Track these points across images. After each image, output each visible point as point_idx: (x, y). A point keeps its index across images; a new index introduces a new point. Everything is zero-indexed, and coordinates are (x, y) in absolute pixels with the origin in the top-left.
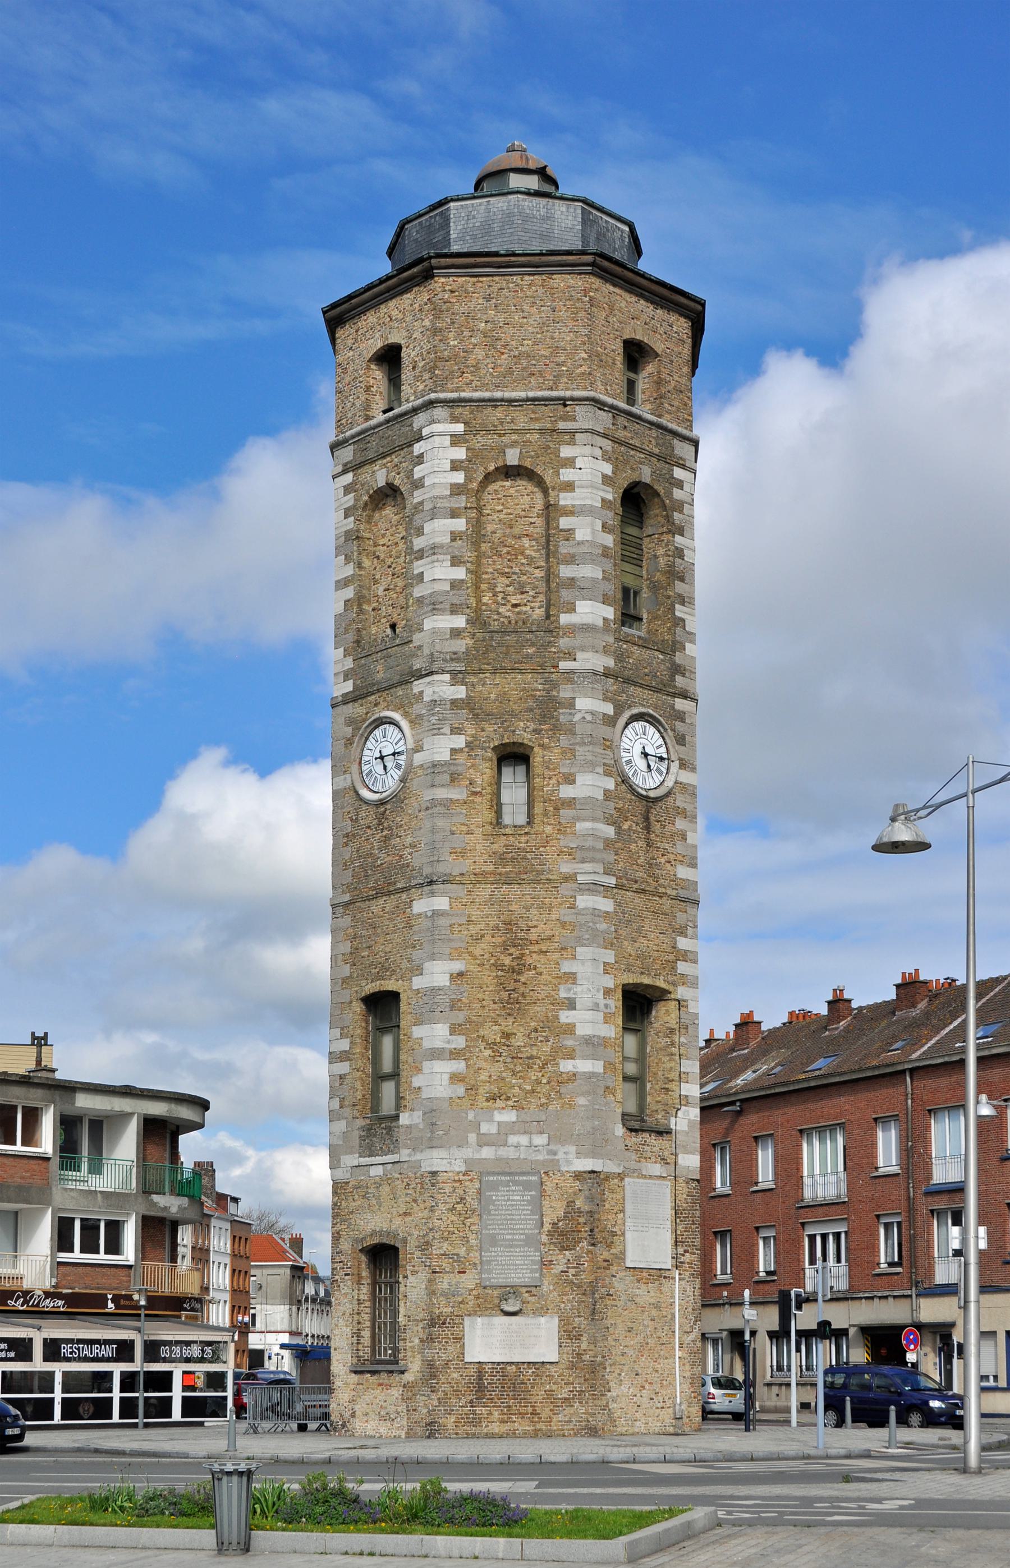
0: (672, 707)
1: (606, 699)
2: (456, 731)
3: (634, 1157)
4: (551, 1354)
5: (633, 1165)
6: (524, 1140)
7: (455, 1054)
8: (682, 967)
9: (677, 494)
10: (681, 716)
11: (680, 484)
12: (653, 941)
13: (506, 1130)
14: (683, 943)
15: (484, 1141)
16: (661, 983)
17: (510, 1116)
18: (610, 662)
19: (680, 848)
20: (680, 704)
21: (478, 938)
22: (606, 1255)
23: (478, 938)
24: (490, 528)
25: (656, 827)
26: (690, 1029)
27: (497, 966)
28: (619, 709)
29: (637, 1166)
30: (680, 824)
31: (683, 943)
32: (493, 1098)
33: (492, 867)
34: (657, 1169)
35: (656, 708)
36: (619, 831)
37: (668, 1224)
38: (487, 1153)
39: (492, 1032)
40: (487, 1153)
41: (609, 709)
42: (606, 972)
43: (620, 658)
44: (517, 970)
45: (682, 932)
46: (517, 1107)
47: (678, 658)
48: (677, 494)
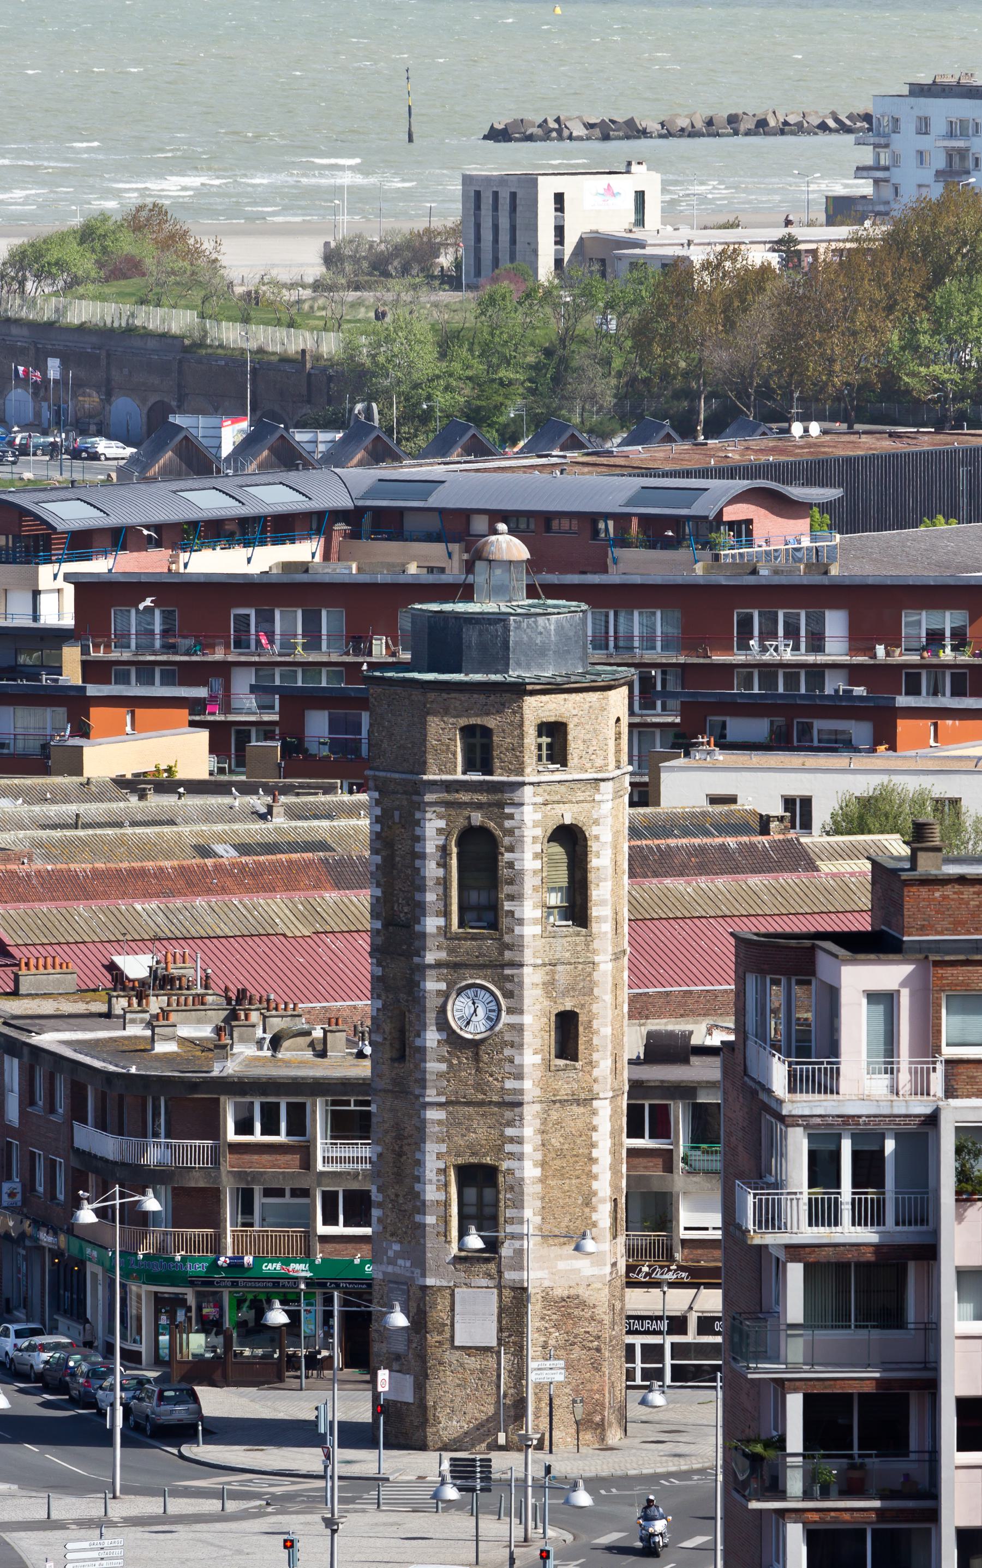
0: (502, 974)
1: (438, 980)
2: (379, 997)
3: (463, 1274)
4: (411, 1400)
5: (463, 1280)
6: (400, 1262)
7: (380, 1205)
8: (508, 1148)
9: (508, 824)
10: (510, 979)
11: (511, 817)
12: (481, 1132)
13: (398, 1255)
14: (509, 1132)
15: (392, 1262)
16: (488, 1160)
17: (396, 1247)
18: (443, 955)
19: (507, 1067)
20: (508, 972)
21: (387, 1132)
22: (438, 1338)
23: (387, 1132)
24: (398, 859)
25: (485, 1058)
26: (516, 1189)
27: (393, 1150)
28: (450, 985)
29: (468, 1281)
30: (507, 1052)
31: (509, 1132)
32: (392, 1235)
33: (390, 1087)
34: (485, 1282)
35: (485, 978)
36: (451, 1065)
37: (495, 1318)
38: (390, 1269)
39: (391, 1192)
40: (390, 1269)
41: (443, 986)
42: (438, 1158)
43: (451, 951)
44: (400, 1154)
45: (510, 1124)
46: (401, 1243)
47: (507, 938)
48: (508, 824)
